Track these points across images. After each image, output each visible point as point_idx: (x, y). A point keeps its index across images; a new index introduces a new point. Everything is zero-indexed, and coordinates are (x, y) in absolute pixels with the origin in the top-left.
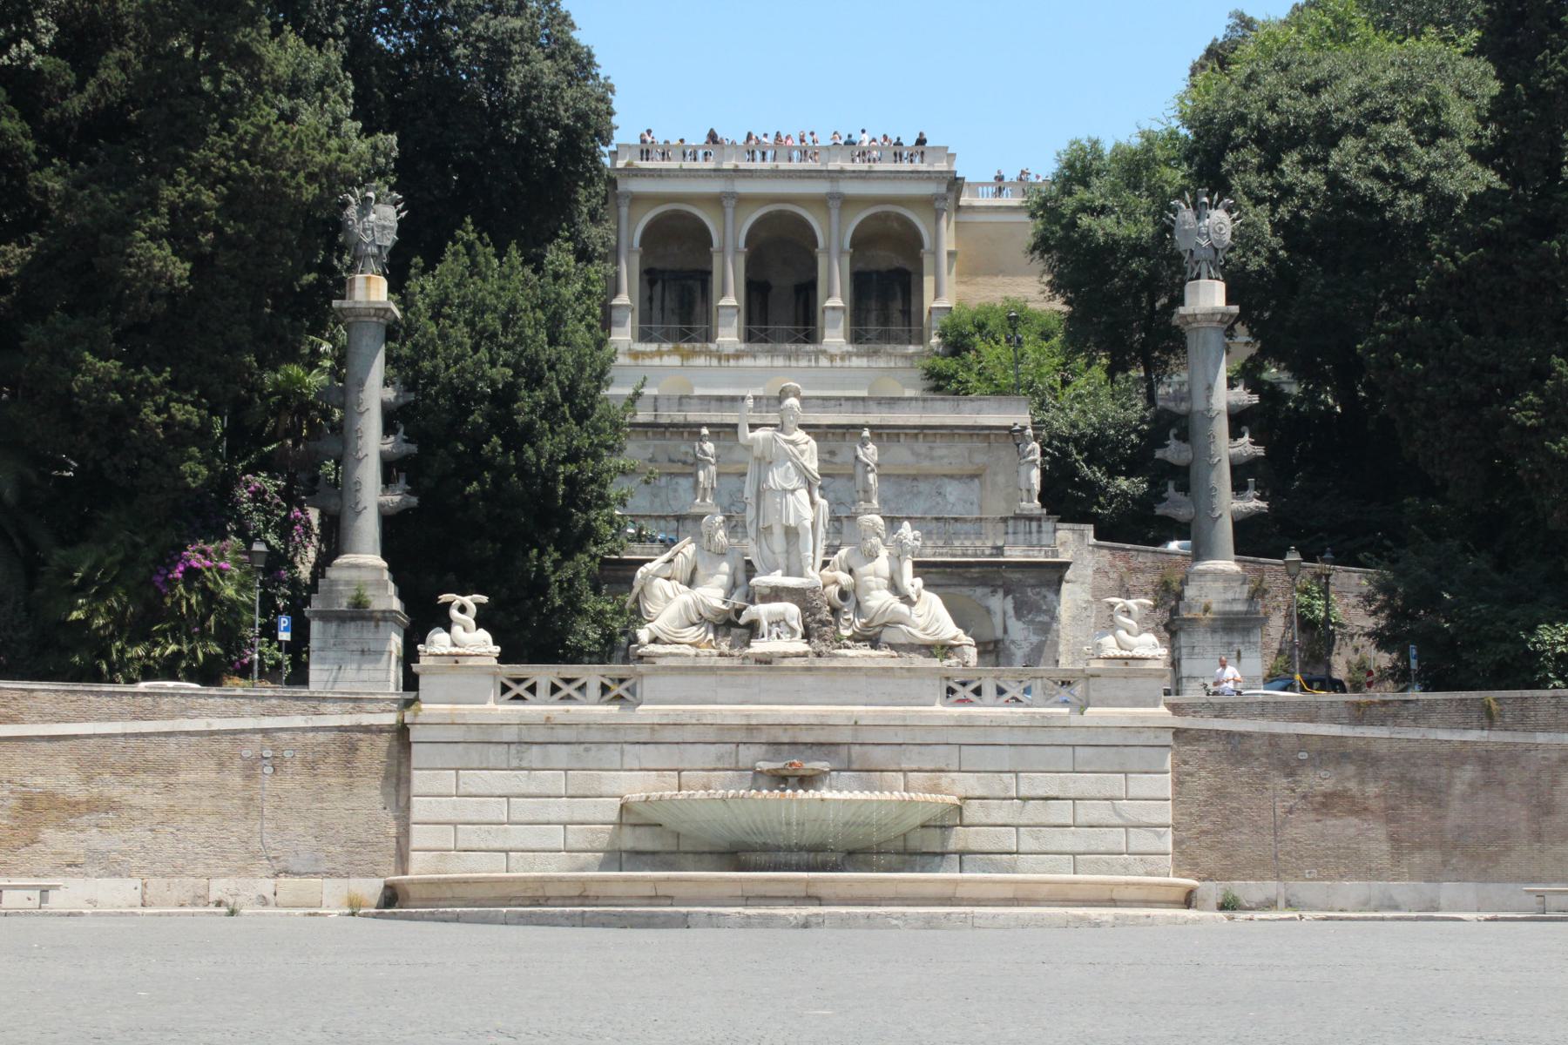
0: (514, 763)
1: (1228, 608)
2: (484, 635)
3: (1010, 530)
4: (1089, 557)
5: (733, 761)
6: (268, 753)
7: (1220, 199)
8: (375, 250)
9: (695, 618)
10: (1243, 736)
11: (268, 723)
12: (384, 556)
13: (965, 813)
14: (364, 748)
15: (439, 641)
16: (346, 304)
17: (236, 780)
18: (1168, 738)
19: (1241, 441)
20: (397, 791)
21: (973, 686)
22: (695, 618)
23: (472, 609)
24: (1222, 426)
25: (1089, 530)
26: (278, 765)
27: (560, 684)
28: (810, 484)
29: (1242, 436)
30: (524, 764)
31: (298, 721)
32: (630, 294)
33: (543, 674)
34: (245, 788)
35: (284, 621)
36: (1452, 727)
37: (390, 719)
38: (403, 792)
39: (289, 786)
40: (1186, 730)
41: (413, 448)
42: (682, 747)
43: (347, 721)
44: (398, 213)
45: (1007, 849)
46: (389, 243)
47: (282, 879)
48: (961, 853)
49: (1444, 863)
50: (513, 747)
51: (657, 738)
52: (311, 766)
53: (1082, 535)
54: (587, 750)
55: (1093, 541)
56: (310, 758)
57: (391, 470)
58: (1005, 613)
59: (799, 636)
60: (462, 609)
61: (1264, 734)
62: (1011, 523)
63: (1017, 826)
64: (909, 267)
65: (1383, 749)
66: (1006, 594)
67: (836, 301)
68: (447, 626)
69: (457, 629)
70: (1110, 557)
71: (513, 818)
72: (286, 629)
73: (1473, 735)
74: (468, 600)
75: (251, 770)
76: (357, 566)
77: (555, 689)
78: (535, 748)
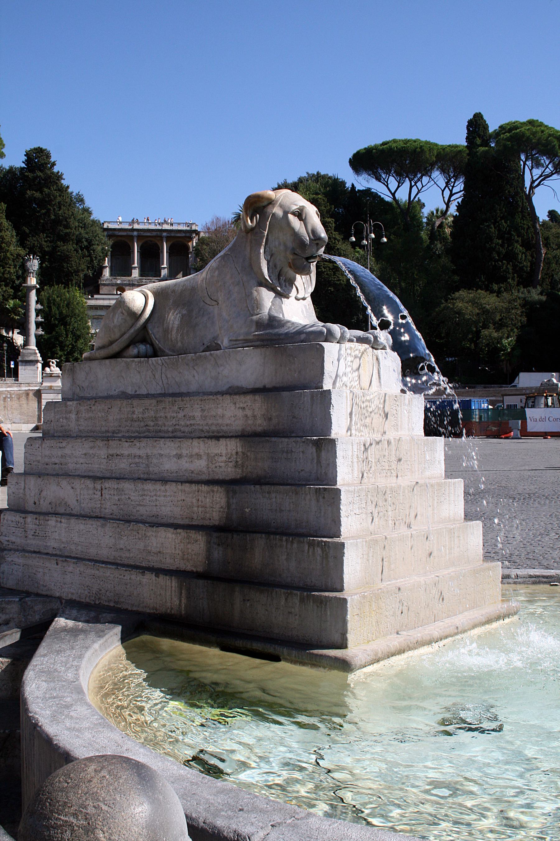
2: (58, 369)
6: (9, 396)
11: (9, 389)
12: (37, 346)
16: (26, 285)
26: (11, 398)
31: (16, 389)
32: (108, 264)
35: (12, 363)
37: (37, 388)
39: (14, 403)
41: (43, 320)
43: (27, 388)
46: (36, 269)
47: (13, 424)
52: (19, 399)
57: (38, 325)
60: (53, 363)
67: (165, 266)
68: (49, 366)
69: (52, 367)
74: (54, 361)
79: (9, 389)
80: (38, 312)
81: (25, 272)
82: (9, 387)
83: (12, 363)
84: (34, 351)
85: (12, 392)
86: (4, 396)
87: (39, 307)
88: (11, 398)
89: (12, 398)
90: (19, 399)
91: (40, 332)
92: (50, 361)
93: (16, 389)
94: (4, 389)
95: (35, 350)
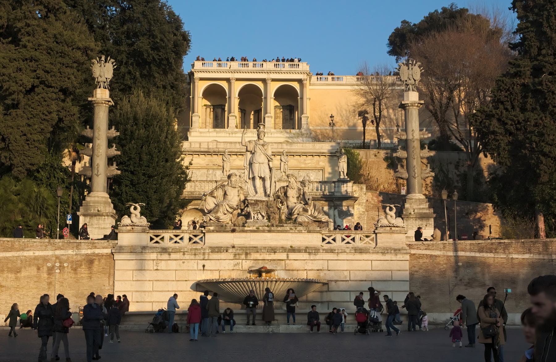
0: (155, 268)
1: (421, 211)
2: (144, 219)
3: (336, 186)
4: (364, 196)
5: (241, 266)
7: (416, 63)
8: (105, 80)
9: (226, 212)
10: (436, 256)
11: (58, 252)
13: (330, 287)
14: (96, 263)
15: (126, 220)
16: (94, 99)
17: (45, 275)
18: (407, 257)
19: (424, 151)
20: (109, 279)
21: (332, 238)
22: (226, 212)
23: (139, 209)
24: (417, 145)
25: (364, 187)
26: (61, 267)
27: (173, 237)
28: (269, 161)
29: (425, 148)
30: (159, 268)
33: (167, 234)
34: (48, 278)
35: (69, 217)
36: (519, 253)
38: (112, 279)
40: (414, 254)
42: (220, 261)
43: (89, 252)
44: (114, 66)
45: (346, 300)
48: (328, 302)
49: (517, 306)
50: (155, 261)
51: (211, 257)
52: (75, 270)
53: (362, 188)
54: (183, 263)
55: (365, 190)
56: (75, 266)
58: (334, 216)
59: (265, 218)
60: (135, 209)
61: (445, 256)
62: (336, 183)
63: (350, 291)
64: (293, 104)
65: (491, 261)
66: (335, 209)
69: (133, 215)
70: (371, 196)
71: (154, 289)
72: (70, 220)
73: (527, 256)
74: (137, 205)
75: (50, 271)
76: (98, 197)
77: (171, 239)
78: (163, 262)
79: (58, 252)
80: (110, 142)
81: (91, 83)
82: (60, 248)
83: (69, 217)
84: (104, 199)
85: (64, 258)
86: (49, 265)
87: (114, 133)
88: (61, 267)
89: (64, 267)
90: (75, 270)
91: (115, 171)
92: (131, 205)
93: (70, 252)
94: (49, 253)
95: (105, 197)
